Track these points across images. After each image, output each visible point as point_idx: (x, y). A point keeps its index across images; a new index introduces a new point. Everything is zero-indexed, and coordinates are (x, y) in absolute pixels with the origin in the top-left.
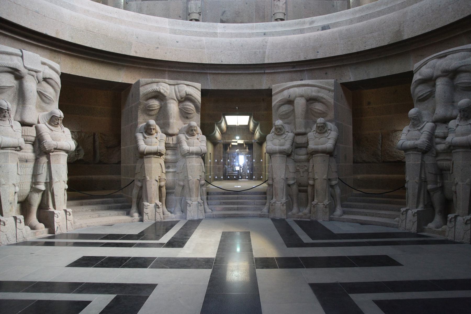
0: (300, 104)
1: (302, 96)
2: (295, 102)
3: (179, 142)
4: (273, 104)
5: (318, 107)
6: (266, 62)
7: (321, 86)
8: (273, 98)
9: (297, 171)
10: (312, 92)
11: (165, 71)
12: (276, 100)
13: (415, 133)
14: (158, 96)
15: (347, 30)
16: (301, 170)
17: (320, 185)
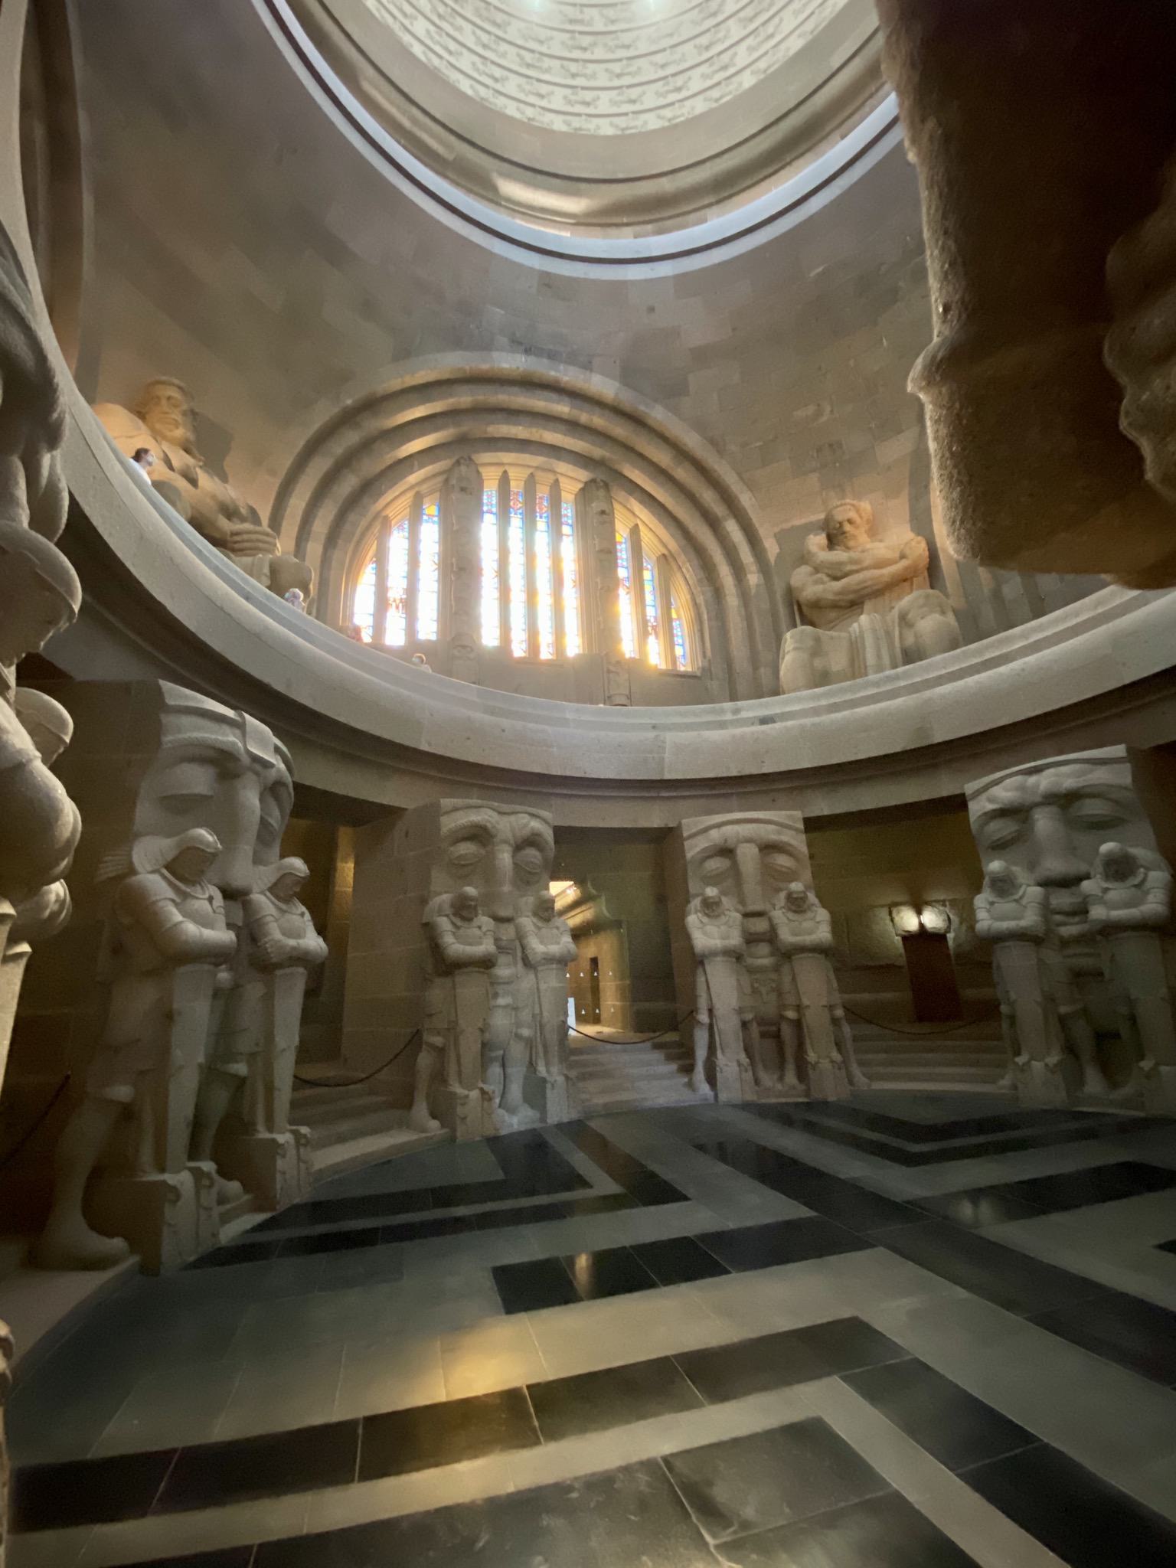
0: (748, 855)
1: (749, 840)
2: (739, 852)
3: (520, 937)
4: (689, 855)
5: (782, 861)
6: (667, 777)
7: (780, 822)
8: (687, 844)
9: (755, 991)
10: (769, 833)
11: (472, 785)
12: (693, 848)
13: (1007, 906)
14: (480, 835)
15: (813, 724)
16: (763, 990)
17: (816, 1019)
